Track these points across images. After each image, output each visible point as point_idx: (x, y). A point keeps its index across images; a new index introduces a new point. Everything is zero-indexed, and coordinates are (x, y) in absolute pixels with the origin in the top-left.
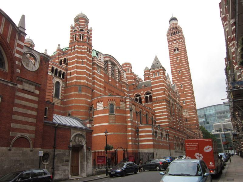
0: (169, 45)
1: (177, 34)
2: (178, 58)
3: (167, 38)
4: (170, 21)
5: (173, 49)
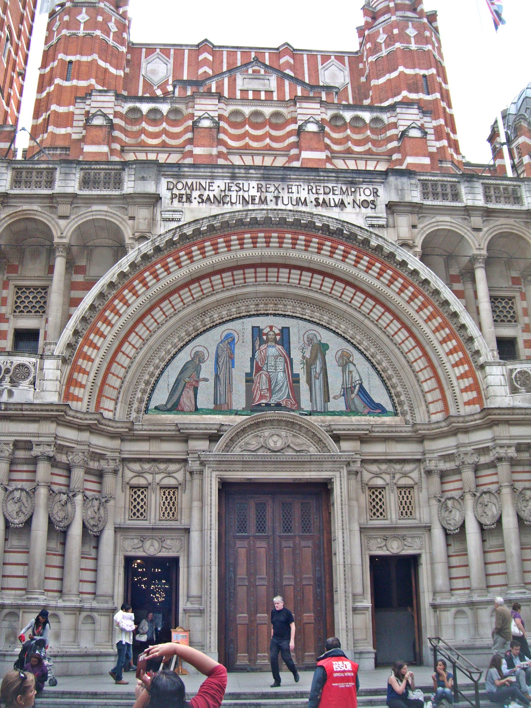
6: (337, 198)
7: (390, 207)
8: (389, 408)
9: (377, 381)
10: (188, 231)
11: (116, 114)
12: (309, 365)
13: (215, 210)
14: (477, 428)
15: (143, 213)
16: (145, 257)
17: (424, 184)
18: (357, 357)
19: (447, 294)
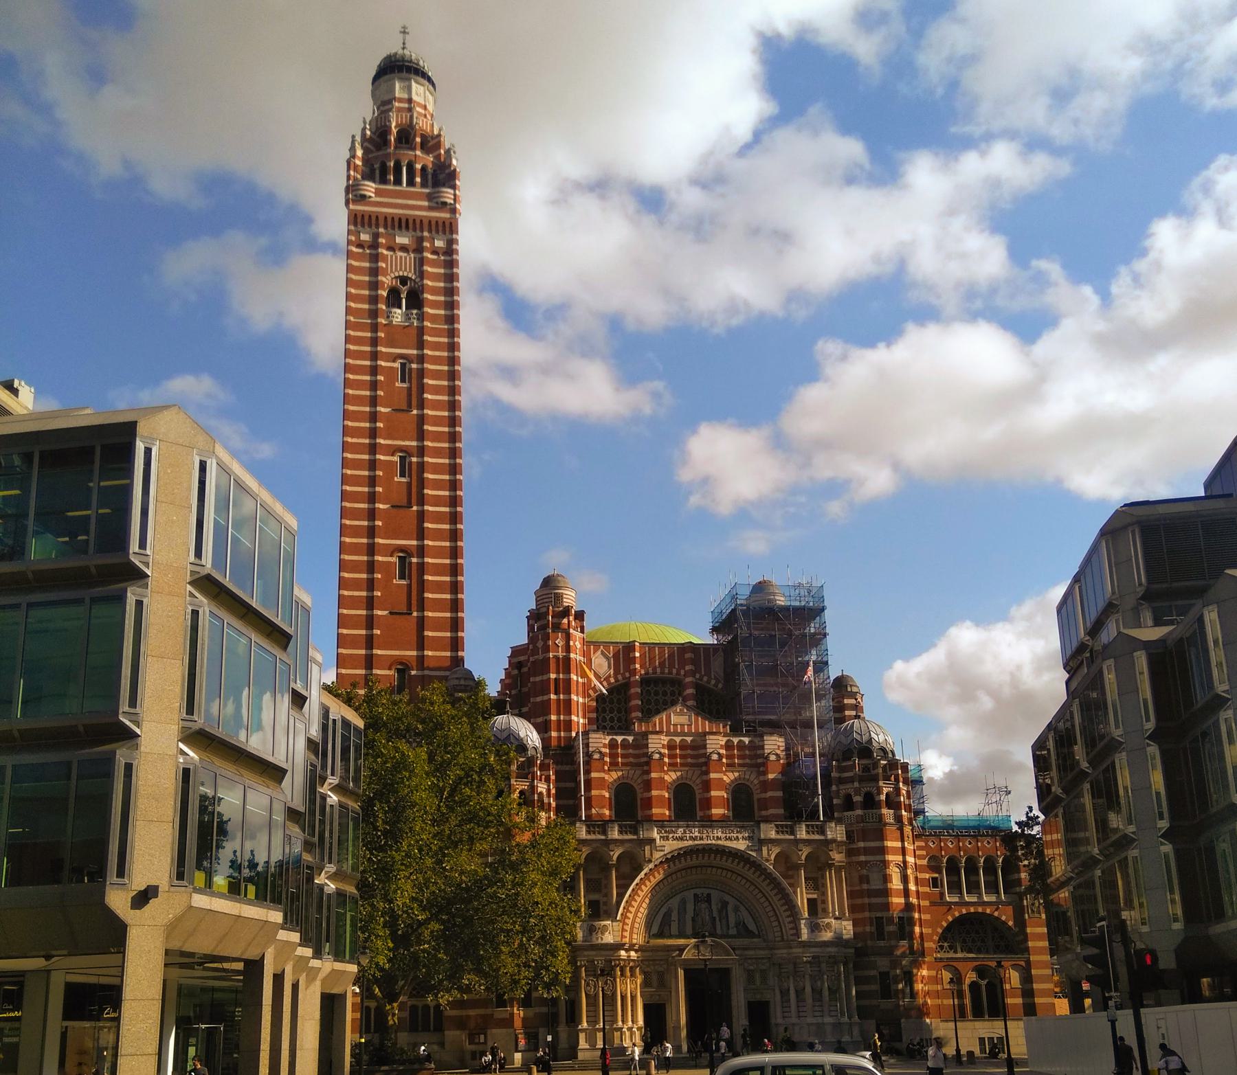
1: (424, 185)
4: (376, 79)
6: (735, 835)
8: (757, 933)
9: (751, 919)
10: (669, 856)
11: (605, 746)
12: (720, 912)
13: (681, 844)
14: (796, 947)
16: (651, 870)
17: (777, 826)
18: (742, 908)
19: (785, 883)
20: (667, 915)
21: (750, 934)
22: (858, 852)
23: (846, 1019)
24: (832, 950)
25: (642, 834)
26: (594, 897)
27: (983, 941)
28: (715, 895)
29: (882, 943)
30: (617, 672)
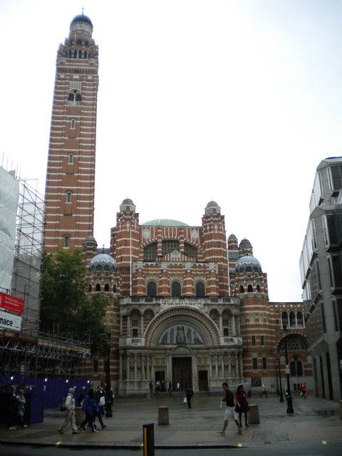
0: (58, 78)
1: (85, 57)
2: (76, 119)
3: (57, 61)
5: (65, 93)
7: (204, 305)
11: (143, 266)
12: (188, 334)
13: (171, 306)
15: (157, 307)
19: (214, 322)
20: (166, 335)
21: (200, 343)
22: (245, 309)
23: (237, 378)
24: (233, 349)
25: (154, 302)
26: (135, 328)
27: (297, 345)
28: (186, 328)
29: (253, 346)
30: (152, 238)
